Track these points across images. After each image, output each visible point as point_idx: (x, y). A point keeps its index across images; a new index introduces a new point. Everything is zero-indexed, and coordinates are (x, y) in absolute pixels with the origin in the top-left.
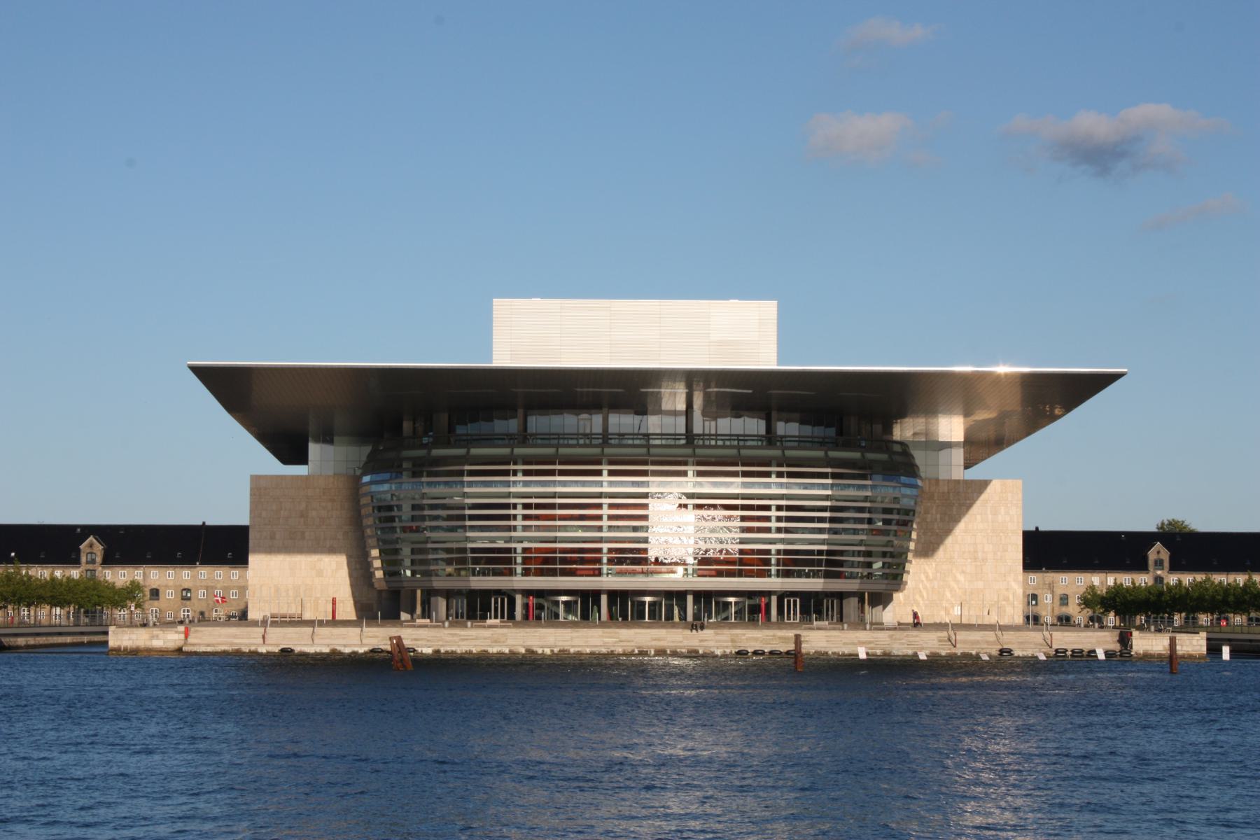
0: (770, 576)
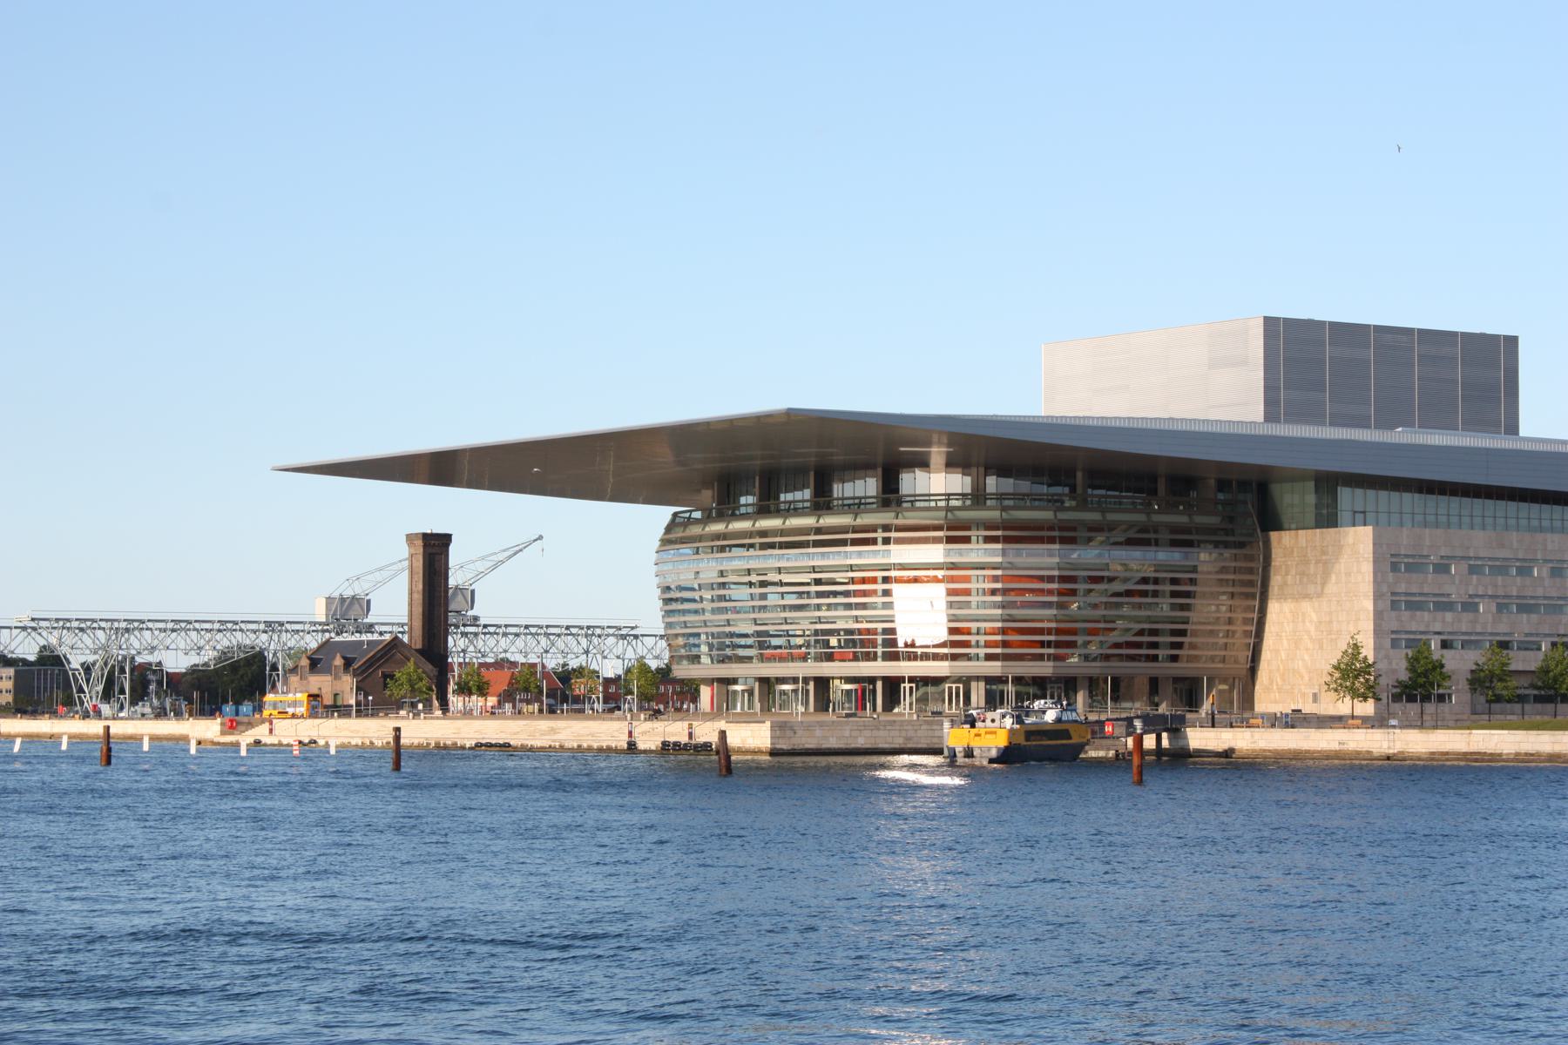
0: (875, 659)
